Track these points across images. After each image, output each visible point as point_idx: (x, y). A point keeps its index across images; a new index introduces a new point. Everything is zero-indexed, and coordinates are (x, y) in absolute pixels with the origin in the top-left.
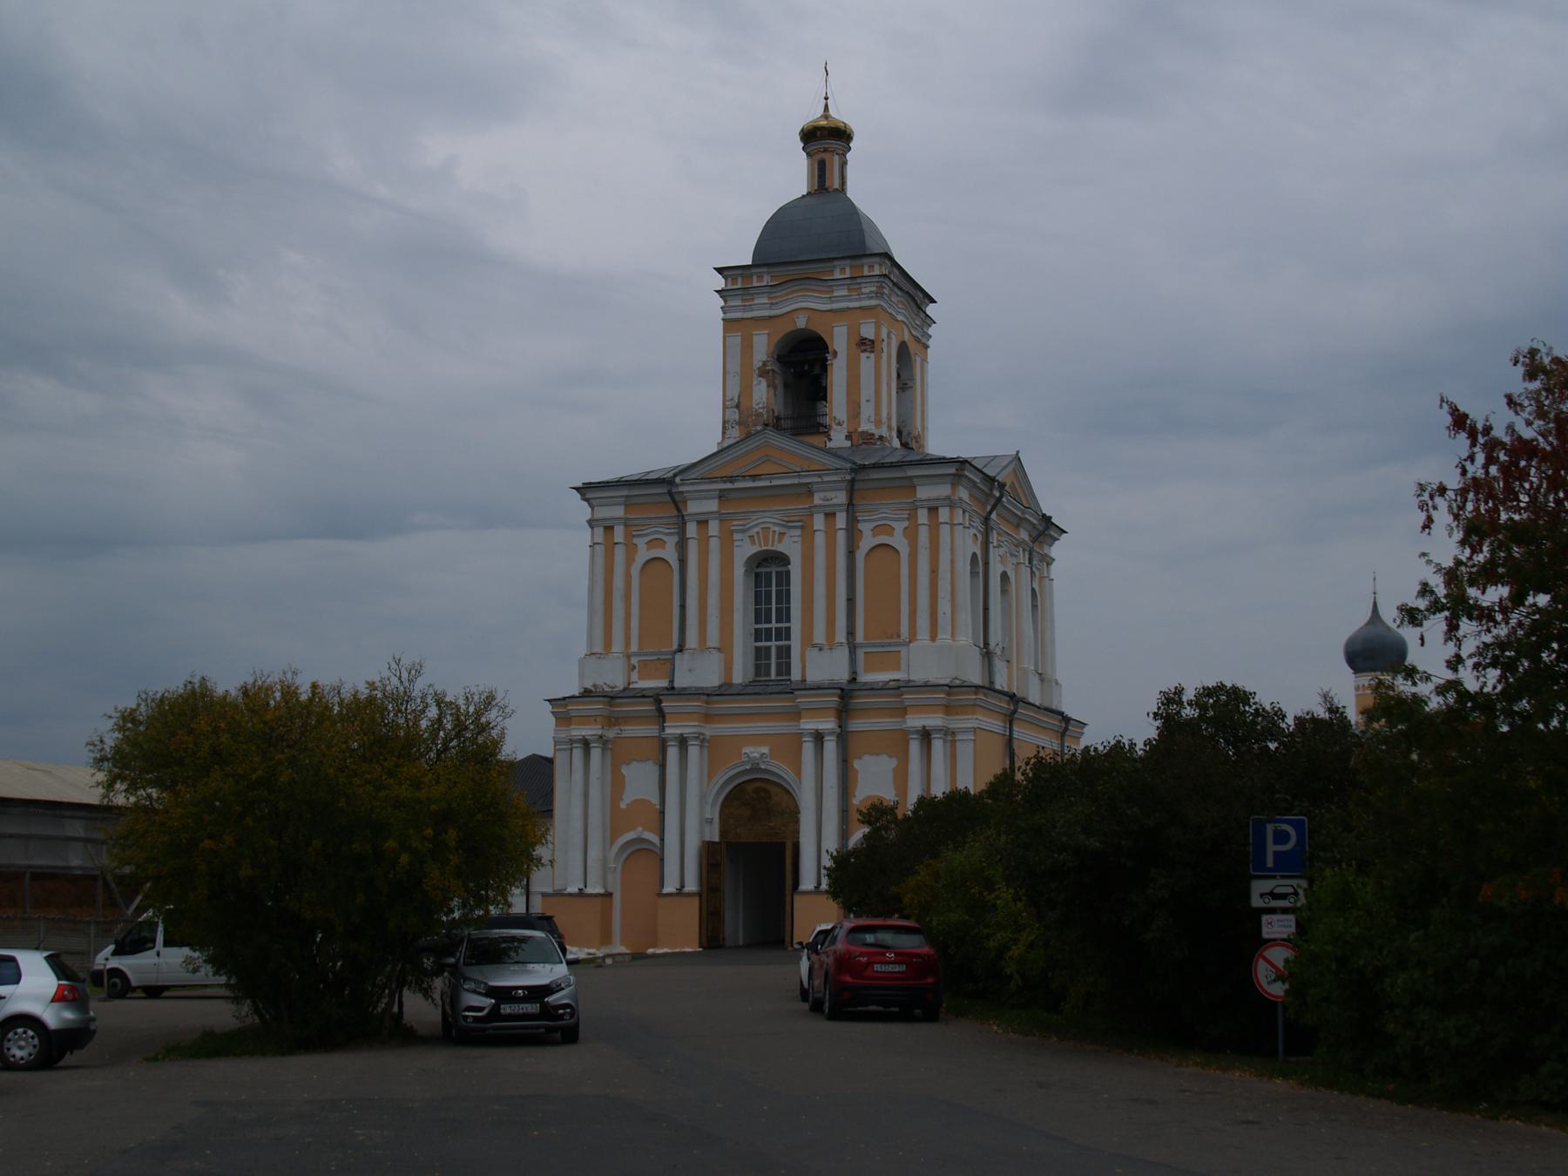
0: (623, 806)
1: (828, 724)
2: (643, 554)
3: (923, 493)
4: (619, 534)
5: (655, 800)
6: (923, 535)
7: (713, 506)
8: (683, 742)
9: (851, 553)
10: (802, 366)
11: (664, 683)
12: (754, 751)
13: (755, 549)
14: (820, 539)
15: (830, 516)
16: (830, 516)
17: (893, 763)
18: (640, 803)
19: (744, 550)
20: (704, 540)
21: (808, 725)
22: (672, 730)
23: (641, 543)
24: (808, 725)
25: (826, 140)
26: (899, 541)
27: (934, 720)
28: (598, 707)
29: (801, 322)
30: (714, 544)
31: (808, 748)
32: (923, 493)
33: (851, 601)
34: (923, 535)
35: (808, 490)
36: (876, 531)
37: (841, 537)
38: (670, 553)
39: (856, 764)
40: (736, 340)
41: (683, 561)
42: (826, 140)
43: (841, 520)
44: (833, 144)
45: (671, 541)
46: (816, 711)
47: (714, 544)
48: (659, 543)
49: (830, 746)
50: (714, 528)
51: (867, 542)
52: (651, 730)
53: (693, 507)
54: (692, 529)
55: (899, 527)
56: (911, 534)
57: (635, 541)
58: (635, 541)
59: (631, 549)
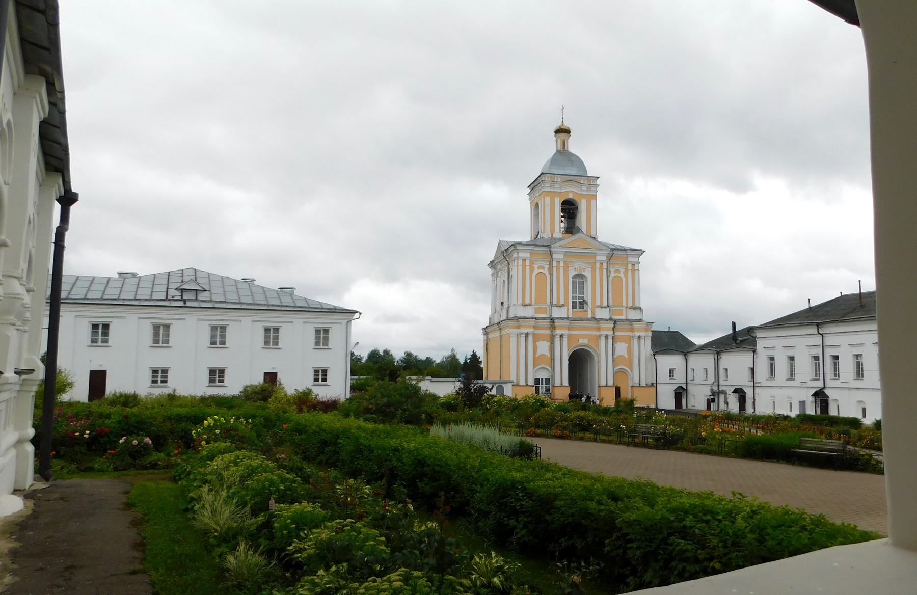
1: (610, 333)
2: (536, 271)
3: (630, 259)
4: (528, 262)
5: (548, 354)
6: (630, 273)
7: (562, 256)
8: (561, 336)
9: (608, 277)
12: (581, 341)
14: (598, 271)
15: (601, 264)
16: (601, 264)
18: (543, 355)
19: (572, 273)
20: (558, 268)
21: (605, 333)
22: (558, 332)
23: (536, 266)
26: (622, 275)
28: (532, 322)
29: (570, 196)
30: (562, 270)
31: (603, 340)
32: (630, 259)
33: (608, 292)
34: (630, 273)
35: (595, 255)
37: (605, 271)
38: (546, 272)
41: (551, 274)
43: (605, 266)
45: (547, 267)
46: (608, 329)
47: (562, 270)
48: (543, 268)
49: (610, 341)
50: (562, 264)
51: (612, 275)
53: (555, 256)
54: (555, 264)
55: (622, 270)
59: (532, 269)
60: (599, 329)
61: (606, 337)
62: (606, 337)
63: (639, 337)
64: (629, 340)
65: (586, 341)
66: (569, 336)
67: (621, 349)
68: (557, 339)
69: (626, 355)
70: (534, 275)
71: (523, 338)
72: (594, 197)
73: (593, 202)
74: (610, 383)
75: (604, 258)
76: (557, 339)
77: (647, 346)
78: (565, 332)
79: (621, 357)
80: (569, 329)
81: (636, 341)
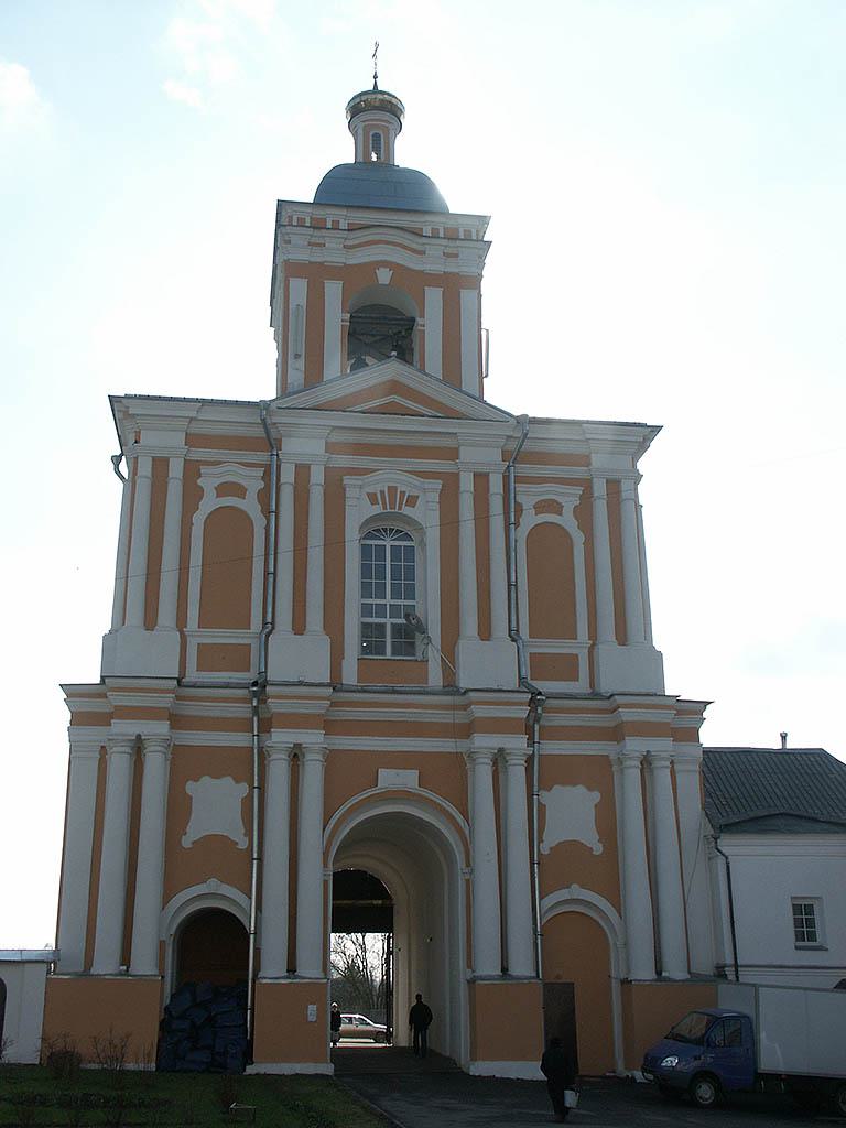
0: (186, 842)
10: (383, 329)
12: (388, 778)
13: (377, 509)
17: (596, 796)
19: (358, 512)
22: (281, 738)
23: (208, 482)
24: (484, 742)
25: (375, 114)
26: (568, 521)
33: (511, 586)
36: (541, 507)
40: (299, 288)
42: (375, 114)
44: (387, 116)
45: (254, 484)
48: (240, 491)
51: (530, 520)
58: (200, 482)
59: (192, 496)
60: (466, 730)
63: (646, 762)
64: (599, 774)
65: (409, 779)
66: (331, 759)
67: (571, 814)
68: (278, 772)
71: (119, 765)
72: (475, 282)
73: (466, 295)
74: (522, 965)
76: (278, 772)
77: (686, 802)
78: (313, 739)
79: (571, 849)
80: (330, 727)
81: (633, 775)
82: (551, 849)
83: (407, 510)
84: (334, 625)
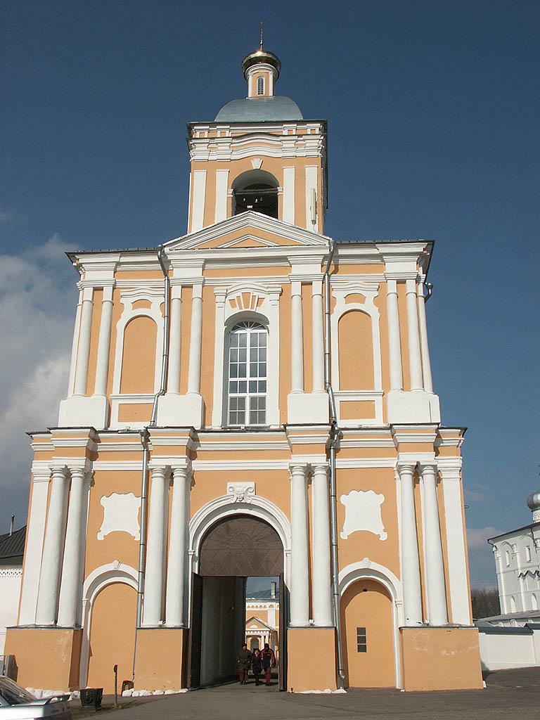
1: (319, 460)
11: (148, 424)
13: (236, 310)
18: (119, 537)
19: (223, 313)
20: (185, 301)
22: (158, 462)
23: (127, 302)
24: (301, 460)
26: (369, 307)
27: (427, 458)
31: (297, 481)
39: (343, 499)
43: (317, 287)
46: (309, 448)
51: (340, 307)
52: (137, 465)
53: (178, 274)
54: (176, 292)
55: (370, 296)
56: (380, 302)
57: (122, 300)
58: (122, 300)
59: (116, 307)
61: (309, 473)
62: (309, 473)
68: (157, 484)
69: (378, 529)
70: (120, 325)
75: (316, 269)
76: (157, 484)
82: (104, 536)
83: (259, 310)
84: (204, 386)
